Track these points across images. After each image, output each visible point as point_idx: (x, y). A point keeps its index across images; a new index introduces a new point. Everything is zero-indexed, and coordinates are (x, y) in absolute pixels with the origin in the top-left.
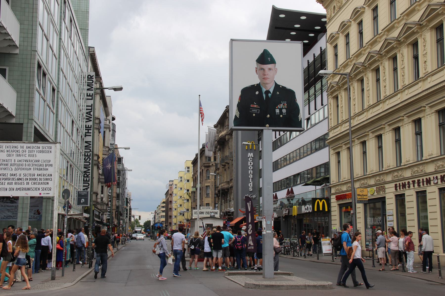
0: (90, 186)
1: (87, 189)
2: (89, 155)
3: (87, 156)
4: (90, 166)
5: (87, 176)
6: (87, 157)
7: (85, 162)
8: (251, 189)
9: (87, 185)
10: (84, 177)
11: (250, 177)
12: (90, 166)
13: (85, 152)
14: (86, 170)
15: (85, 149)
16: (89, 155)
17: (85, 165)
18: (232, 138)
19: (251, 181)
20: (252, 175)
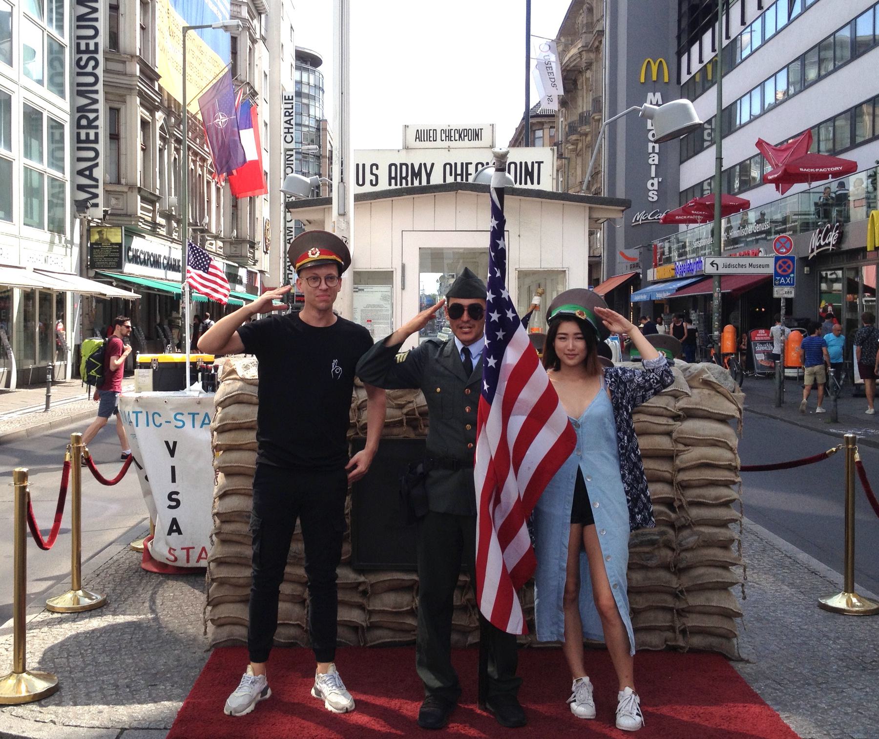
0: (101, 160)
1: (91, 169)
2: (92, 47)
3: (87, 51)
4: (100, 87)
5: (91, 125)
6: (85, 57)
7: (79, 74)
8: (653, 196)
9: (92, 154)
10: (79, 126)
11: (650, 161)
12: (100, 87)
13: (79, 38)
14: (83, 101)
15: (79, 27)
16: (92, 47)
17: (79, 85)
18: (597, 60)
19: (653, 175)
20: (656, 157)
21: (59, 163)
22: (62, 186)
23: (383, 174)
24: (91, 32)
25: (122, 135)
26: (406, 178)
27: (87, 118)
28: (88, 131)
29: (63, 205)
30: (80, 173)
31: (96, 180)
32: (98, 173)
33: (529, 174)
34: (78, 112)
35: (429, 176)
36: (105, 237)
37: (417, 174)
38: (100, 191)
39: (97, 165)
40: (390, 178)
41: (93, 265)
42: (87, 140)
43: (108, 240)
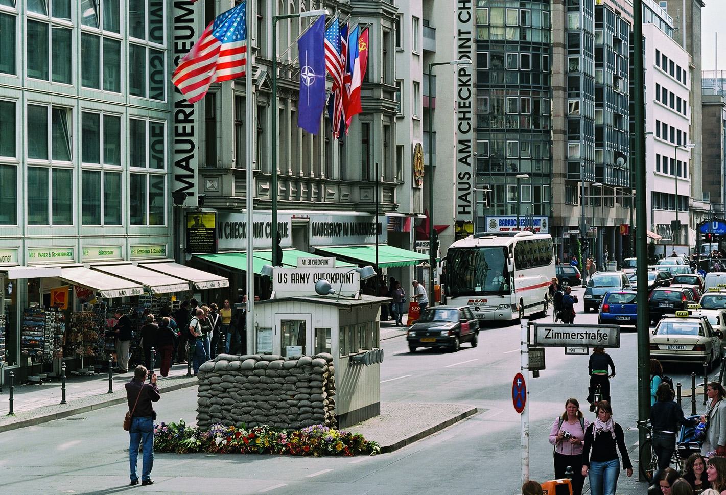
1: (187, 160)
2: (188, 47)
5: (187, 119)
9: (187, 146)
13: (178, 38)
21: (159, 155)
22: (162, 177)
23: (289, 278)
24: (187, 33)
25: (218, 119)
26: (298, 280)
27: (184, 112)
28: (184, 124)
29: (162, 195)
30: (178, 164)
31: (192, 171)
32: (194, 164)
33: (348, 279)
34: (176, 107)
35: (308, 279)
36: (200, 222)
37: (303, 278)
38: (195, 181)
39: (192, 156)
40: (292, 280)
41: (189, 250)
42: (185, 134)
43: (203, 225)
